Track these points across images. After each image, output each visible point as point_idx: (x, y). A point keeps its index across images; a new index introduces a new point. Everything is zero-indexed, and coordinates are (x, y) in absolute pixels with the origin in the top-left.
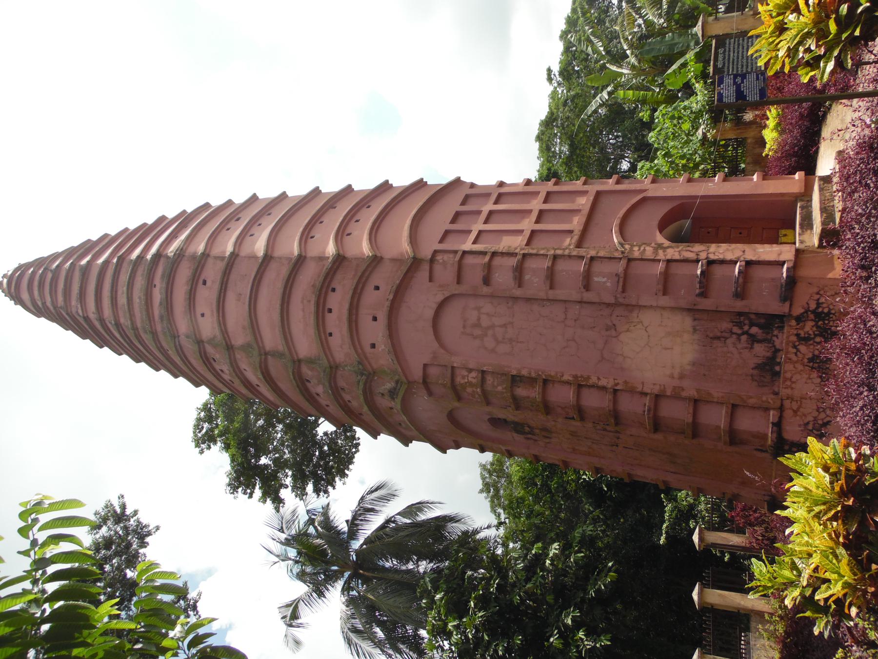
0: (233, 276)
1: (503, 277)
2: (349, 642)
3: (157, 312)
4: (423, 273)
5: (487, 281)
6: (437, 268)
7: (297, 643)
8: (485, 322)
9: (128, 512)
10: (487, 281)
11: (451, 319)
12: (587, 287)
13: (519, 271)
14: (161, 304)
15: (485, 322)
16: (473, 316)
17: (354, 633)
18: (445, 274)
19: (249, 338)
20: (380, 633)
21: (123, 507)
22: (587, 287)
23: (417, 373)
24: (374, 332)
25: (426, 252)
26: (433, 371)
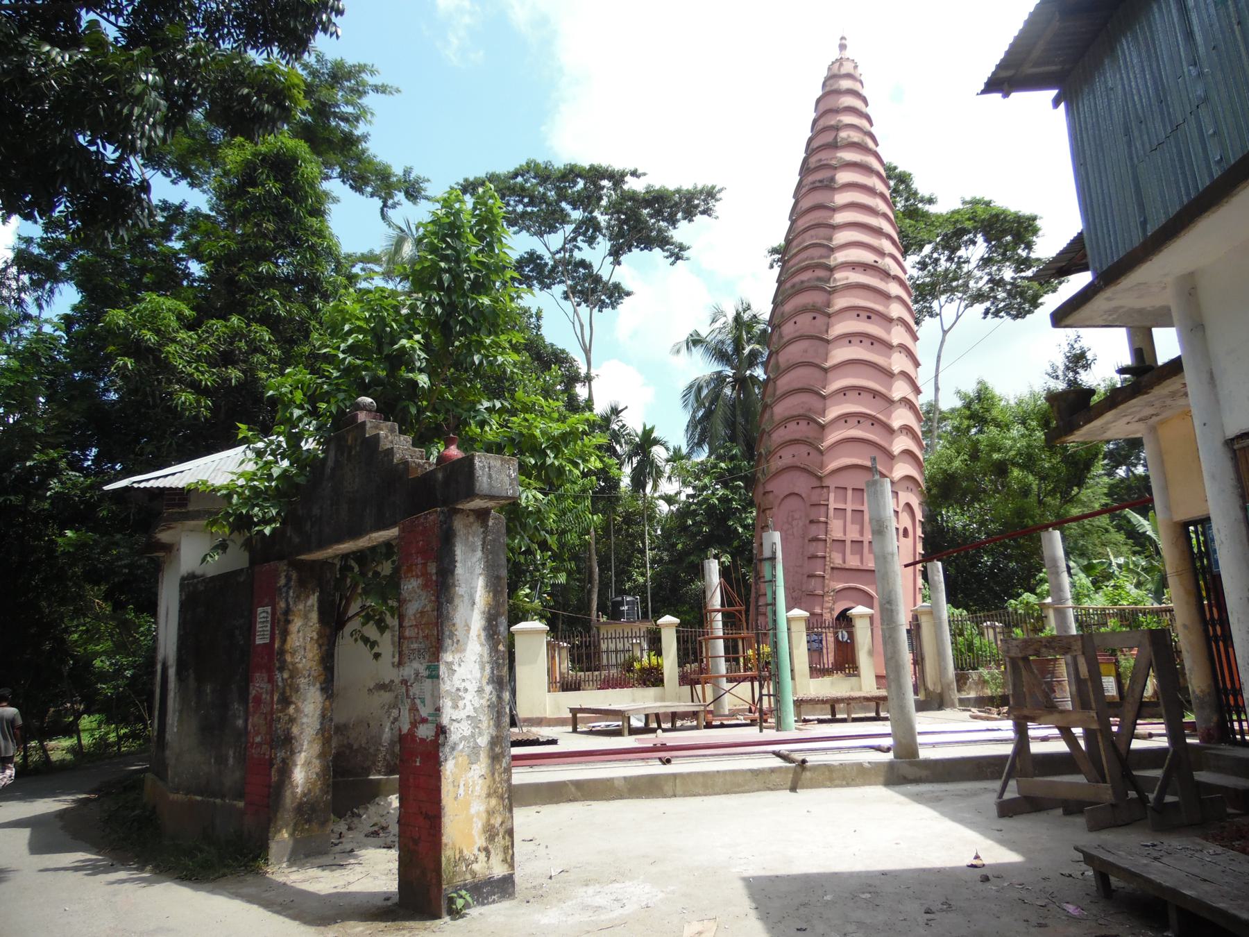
0: (817, 342)
1: (814, 530)
2: (691, 387)
3: (797, 279)
4: (816, 483)
5: (812, 522)
6: (818, 490)
7: (678, 351)
8: (795, 523)
9: (718, 196)
10: (812, 522)
11: (793, 503)
12: (809, 576)
13: (815, 540)
14: (802, 282)
15: (795, 523)
16: (797, 516)
17: (695, 389)
18: (815, 498)
19: (783, 366)
20: (700, 413)
21: (720, 191)
22: (809, 576)
23: (769, 488)
24: (786, 457)
25: (826, 482)
26: (771, 496)
